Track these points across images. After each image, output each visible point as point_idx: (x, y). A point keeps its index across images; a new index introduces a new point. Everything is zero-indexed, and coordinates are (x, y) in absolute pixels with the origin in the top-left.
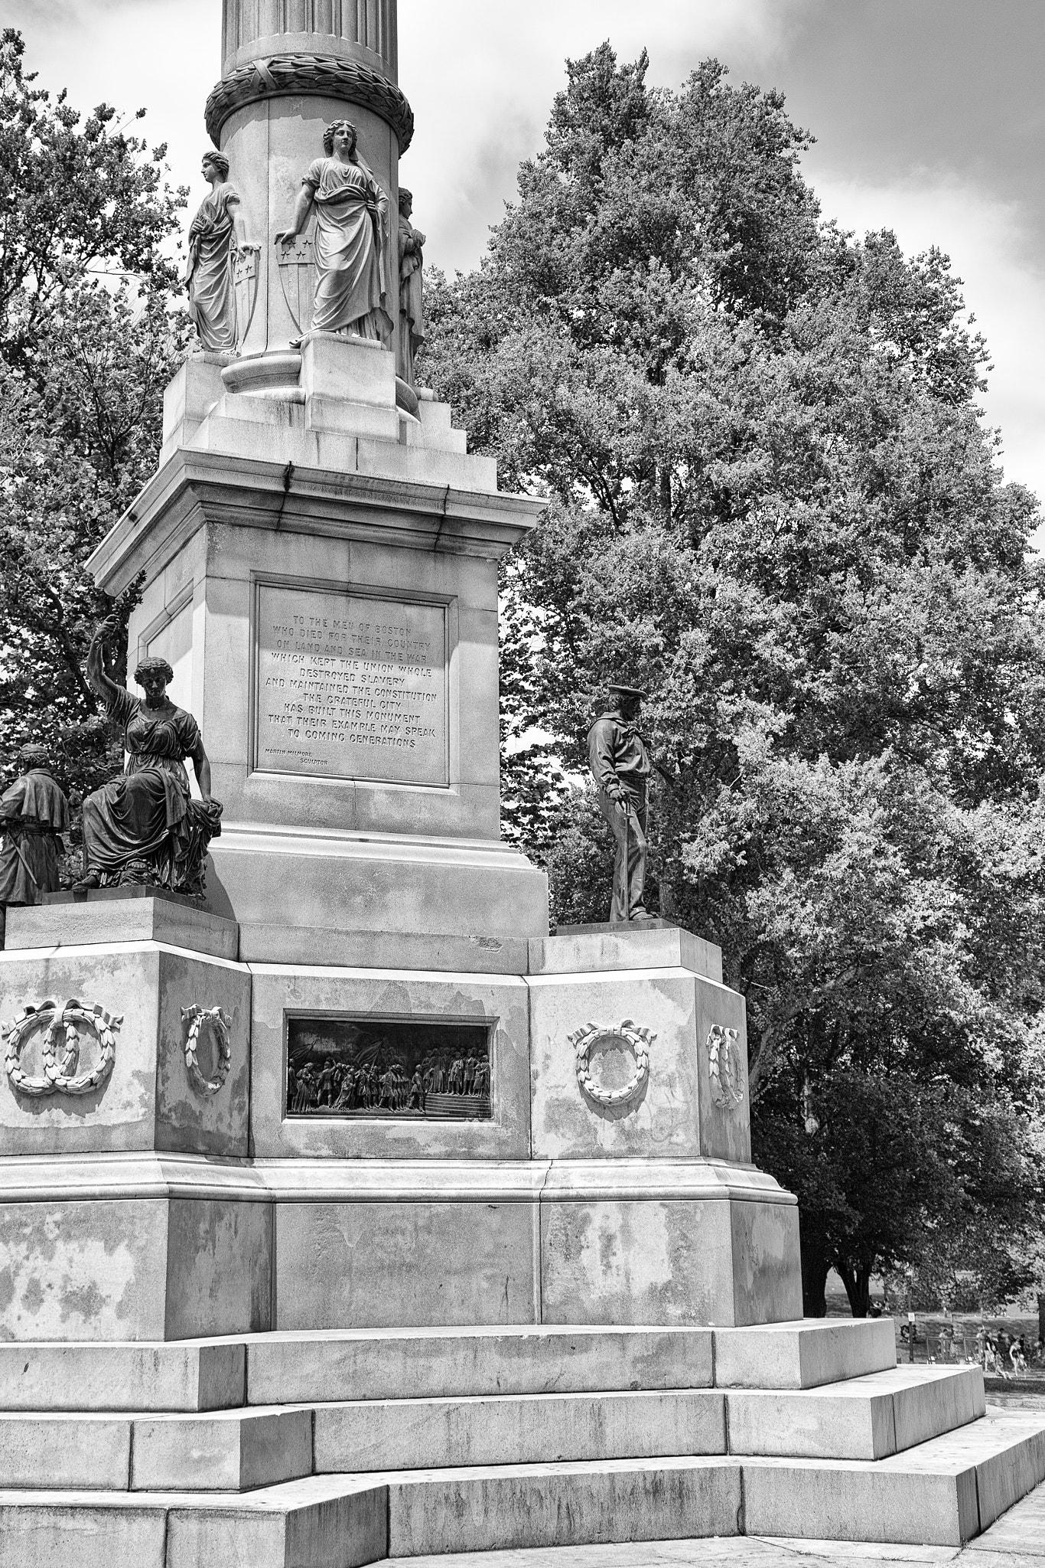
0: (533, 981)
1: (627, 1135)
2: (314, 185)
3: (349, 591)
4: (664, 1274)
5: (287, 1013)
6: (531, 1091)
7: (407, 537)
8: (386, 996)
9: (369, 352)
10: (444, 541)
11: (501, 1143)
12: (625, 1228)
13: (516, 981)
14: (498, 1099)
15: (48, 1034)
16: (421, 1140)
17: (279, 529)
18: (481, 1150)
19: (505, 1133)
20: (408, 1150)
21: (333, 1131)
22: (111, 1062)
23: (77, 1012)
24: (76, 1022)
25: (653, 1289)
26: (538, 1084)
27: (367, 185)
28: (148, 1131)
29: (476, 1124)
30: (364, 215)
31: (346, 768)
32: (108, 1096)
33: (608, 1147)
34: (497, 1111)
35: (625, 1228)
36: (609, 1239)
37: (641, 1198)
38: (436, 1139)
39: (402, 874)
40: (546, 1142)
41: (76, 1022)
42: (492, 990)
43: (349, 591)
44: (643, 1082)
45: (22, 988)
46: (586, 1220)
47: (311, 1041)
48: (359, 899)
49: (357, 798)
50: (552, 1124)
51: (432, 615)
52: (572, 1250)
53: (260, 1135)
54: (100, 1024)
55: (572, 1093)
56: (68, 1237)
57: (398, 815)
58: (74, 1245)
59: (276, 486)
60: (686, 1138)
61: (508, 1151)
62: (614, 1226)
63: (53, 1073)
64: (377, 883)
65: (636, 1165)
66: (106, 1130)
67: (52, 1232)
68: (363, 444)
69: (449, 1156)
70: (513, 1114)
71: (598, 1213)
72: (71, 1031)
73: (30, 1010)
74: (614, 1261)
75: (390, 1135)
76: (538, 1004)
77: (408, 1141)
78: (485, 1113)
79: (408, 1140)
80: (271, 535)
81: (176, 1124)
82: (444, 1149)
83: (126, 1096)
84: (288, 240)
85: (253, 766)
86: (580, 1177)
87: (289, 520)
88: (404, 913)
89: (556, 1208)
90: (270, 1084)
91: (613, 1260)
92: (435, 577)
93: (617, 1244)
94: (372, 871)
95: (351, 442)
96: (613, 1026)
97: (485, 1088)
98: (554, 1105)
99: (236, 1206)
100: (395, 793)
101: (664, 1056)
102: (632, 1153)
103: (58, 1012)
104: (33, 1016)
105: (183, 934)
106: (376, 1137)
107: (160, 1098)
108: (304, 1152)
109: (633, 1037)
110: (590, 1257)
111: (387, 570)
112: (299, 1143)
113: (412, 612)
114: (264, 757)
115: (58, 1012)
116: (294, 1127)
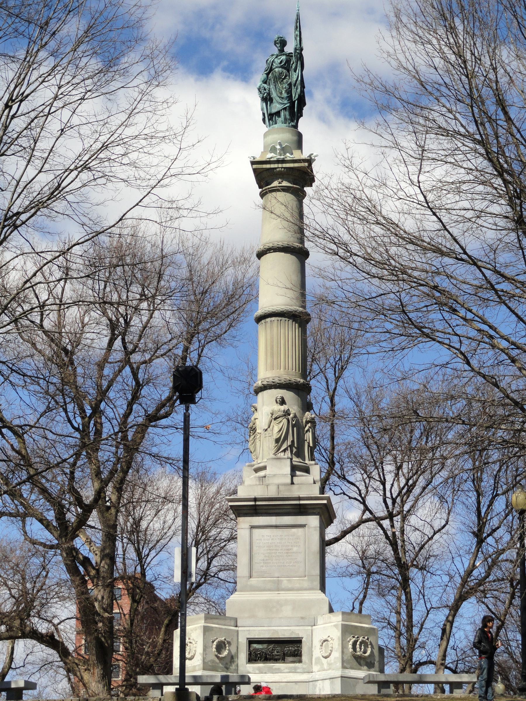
0: (314, 627)
1: (329, 664)
2: (272, 414)
3: (276, 527)
7: (291, 511)
9: (282, 460)
10: (302, 510)
11: (304, 669)
12: (323, 687)
13: (310, 628)
14: (304, 658)
16: (282, 669)
18: (298, 671)
19: (305, 666)
20: (279, 671)
21: (259, 667)
22: (195, 651)
26: (314, 654)
28: (202, 666)
31: (277, 575)
35: (323, 687)
39: (286, 602)
40: (315, 668)
43: (276, 527)
44: (331, 651)
46: (316, 686)
48: (275, 609)
49: (279, 582)
50: (316, 663)
57: (290, 586)
60: (339, 664)
61: (306, 671)
64: (280, 604)
66: (195, 666)
68: (280, 487)
69: (289, 672)
70: (307, 661)
77: (279, 669)
78: (300, 661)
84: (266, 430)
85: (251, 577)
87: (259, 511)
88: (287, 611)
90: (243, 656)
94: (278, 602)
95: (276, 487)
97: (300, 655)
98: (316, 659)
106: (271, 668)
107: (204, 659)
109: (329, 639)
114: (254, 574)
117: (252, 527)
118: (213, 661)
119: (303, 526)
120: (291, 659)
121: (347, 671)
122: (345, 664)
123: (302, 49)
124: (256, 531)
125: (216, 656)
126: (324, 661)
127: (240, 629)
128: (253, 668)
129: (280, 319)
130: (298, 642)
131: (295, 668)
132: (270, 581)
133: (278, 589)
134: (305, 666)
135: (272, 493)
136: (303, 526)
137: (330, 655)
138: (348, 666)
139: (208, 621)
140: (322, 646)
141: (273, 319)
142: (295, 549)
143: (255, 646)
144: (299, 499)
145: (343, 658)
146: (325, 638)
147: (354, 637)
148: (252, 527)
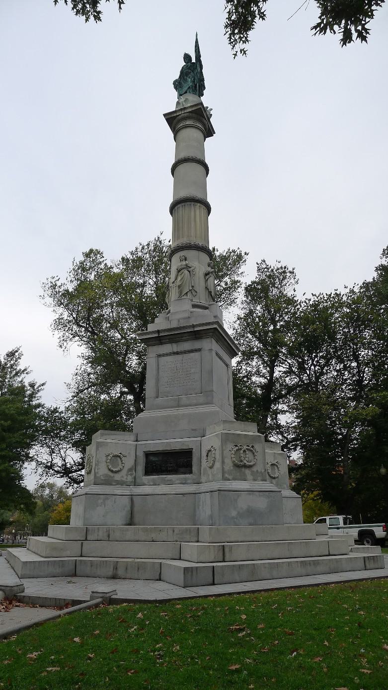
2: (177, 270)
3: (177, 353)
10: (197, 336)
13: (199, 439)
14: (194, 469)
16: (174, 480)
17: (162, 344)
18: (189, 481)
20: (171, 483)
21: (153, 479)
27: (186, 265)
29: (187, 476)
30: (186, 272)
34: (193, 472)
38: (177, 480)
40: (203, 479)
43: (177, 353)
47: (152, 458)
53: (138, 481)
59: (156, 335)
60: (220, 476)
61: (195, 482)
68: (180, 320)
78: (191, 472)
79: (170, 480)
80: (160, 346)
81: (103, 479)
82: (179, 482)
85: (157, 397)
92: (197, 344)
99: (115, 496)
105: (107, 437)
108: (147, 484)
109: (212, 450)
110: (200, 508)
111: (186, 346)
112: (146, 482)
113: (192, 354)
117: (159, 356)
118: (106, 475)
119: (199, 350)
120: (182, 470)
121: (227, 483)
122: (226, 475)
123: (200, 56)
124: (163, 360)
125: (109, 470)
126: (209, 471)
127: (139, 443)
129: (183, 204)
131: (186, 479)
133: (179, 406)
135: (174, 325)
136: (199, 350)
137: (213, 465)
138: (230, 477)
139: (105, 437)
140: (207, 456)
141: (179, 206)
142: (192, 371)
143: (152, 458)
144: (194, 326)
145: (223, 469)
146: (209, 448)
147: (236, 446)
148: (159, 356)
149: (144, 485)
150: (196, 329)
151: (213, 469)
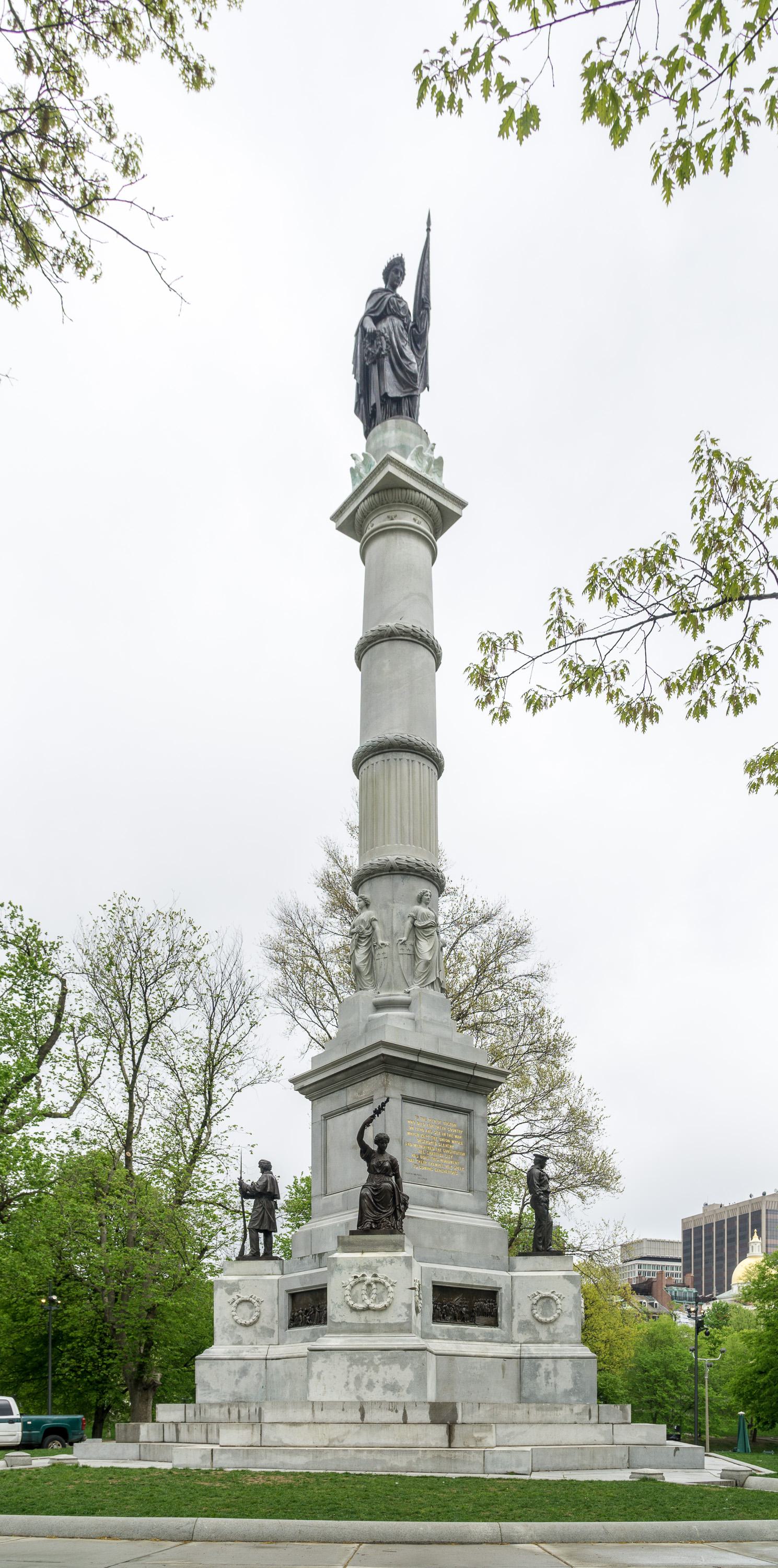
3: (435, 1105)
4: (570, 1386)
5: (433, 1282)
6: (513, 1317)
8: (465, 1277)
13: (505, 1274)
15: (364, 1287)
16: (477, 1334)
18: (496, 1339)
19: (503, 1332)
20: (472, 1338)
21: (448, 1329)
23: (377, 1279)
24: (376, 1282)
25: (566, 1391)
26: (515, 1314)
29: (493, 1329)
32: (391, 1311)
33: (544, 1339)
35: (555, 1370)
36: (548, 1374)
37: (561, 1358)
41: (376, 1282)
42: (499, 1277)
45: (351, 1268)
46: (539, 1366)
49: (438, 1195)
50: (521, 1330)
51: (462, 1119)
52: (534, 1376)
54: (387, 1284)
55: (529, 1317)
56: (384, 1364)
58: (387, 1367)
60: (577, 1336)
62: (551, 1368)
63: (368, 1302)
65: (556, 1346)
67: (377, 1362)
70: (506, 1326)
71: (544, 1364)
72: (374, 1286)
73: (356, 1277)
74: (550, 1381)
75: (467, 1332)
76: (516, 1283)
78: (496, 1324)
83: (399, 1312)
86: (534, 1350)
89: (526, 1361)
91: (550, 1381)
92: (465, 1101)
93: (552, 1375)
96: (547, 1293)
98: (520, 1323)
100: (451, 1194)
101: (567, 1305)
102: (553, 1342)
103: (369, 1278)
104: (357, 1280)
110: (541, 1380)
112: (437, 1333)
113: (455, 1116)
115: (369, 1278)
116: (436, 1328)
117: (405, 1099)
119: (468, 1112)
120: (483, 1319)
128: (442, 1331)
130: (492, 1295)
132: (429, 1191)
134: (503, 1332)
136: (468, 1112)
137: (556, 1320)
149: (435, 1337)
150: (477, 1074)
151: (552, 1327)
